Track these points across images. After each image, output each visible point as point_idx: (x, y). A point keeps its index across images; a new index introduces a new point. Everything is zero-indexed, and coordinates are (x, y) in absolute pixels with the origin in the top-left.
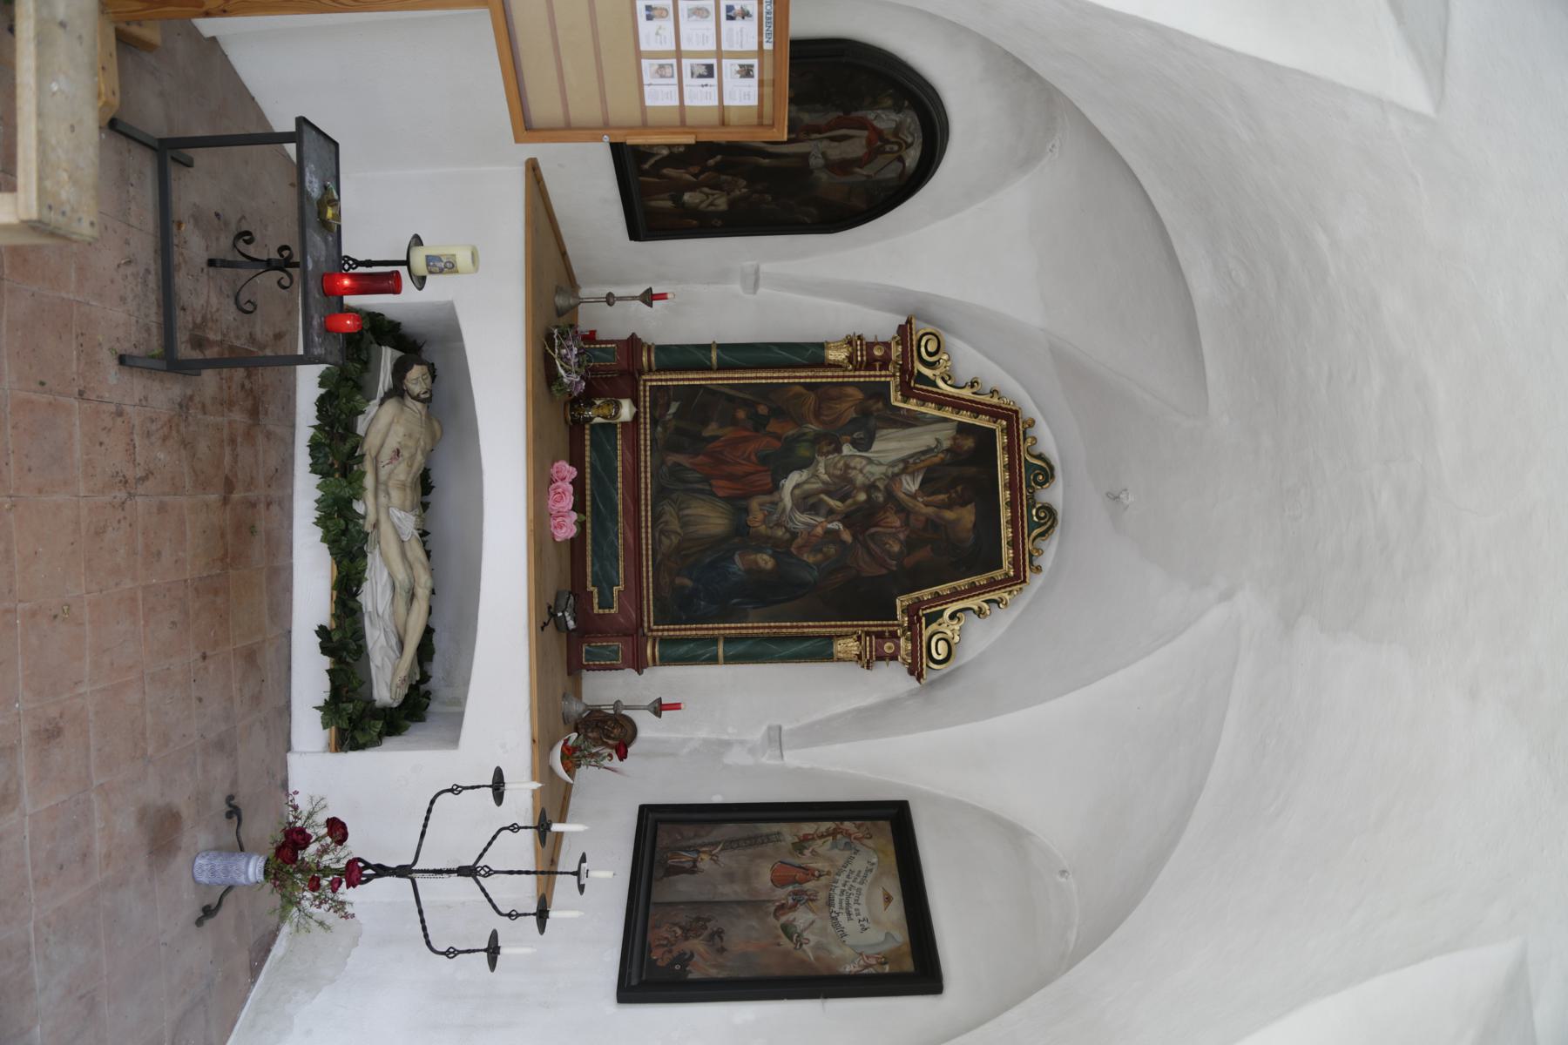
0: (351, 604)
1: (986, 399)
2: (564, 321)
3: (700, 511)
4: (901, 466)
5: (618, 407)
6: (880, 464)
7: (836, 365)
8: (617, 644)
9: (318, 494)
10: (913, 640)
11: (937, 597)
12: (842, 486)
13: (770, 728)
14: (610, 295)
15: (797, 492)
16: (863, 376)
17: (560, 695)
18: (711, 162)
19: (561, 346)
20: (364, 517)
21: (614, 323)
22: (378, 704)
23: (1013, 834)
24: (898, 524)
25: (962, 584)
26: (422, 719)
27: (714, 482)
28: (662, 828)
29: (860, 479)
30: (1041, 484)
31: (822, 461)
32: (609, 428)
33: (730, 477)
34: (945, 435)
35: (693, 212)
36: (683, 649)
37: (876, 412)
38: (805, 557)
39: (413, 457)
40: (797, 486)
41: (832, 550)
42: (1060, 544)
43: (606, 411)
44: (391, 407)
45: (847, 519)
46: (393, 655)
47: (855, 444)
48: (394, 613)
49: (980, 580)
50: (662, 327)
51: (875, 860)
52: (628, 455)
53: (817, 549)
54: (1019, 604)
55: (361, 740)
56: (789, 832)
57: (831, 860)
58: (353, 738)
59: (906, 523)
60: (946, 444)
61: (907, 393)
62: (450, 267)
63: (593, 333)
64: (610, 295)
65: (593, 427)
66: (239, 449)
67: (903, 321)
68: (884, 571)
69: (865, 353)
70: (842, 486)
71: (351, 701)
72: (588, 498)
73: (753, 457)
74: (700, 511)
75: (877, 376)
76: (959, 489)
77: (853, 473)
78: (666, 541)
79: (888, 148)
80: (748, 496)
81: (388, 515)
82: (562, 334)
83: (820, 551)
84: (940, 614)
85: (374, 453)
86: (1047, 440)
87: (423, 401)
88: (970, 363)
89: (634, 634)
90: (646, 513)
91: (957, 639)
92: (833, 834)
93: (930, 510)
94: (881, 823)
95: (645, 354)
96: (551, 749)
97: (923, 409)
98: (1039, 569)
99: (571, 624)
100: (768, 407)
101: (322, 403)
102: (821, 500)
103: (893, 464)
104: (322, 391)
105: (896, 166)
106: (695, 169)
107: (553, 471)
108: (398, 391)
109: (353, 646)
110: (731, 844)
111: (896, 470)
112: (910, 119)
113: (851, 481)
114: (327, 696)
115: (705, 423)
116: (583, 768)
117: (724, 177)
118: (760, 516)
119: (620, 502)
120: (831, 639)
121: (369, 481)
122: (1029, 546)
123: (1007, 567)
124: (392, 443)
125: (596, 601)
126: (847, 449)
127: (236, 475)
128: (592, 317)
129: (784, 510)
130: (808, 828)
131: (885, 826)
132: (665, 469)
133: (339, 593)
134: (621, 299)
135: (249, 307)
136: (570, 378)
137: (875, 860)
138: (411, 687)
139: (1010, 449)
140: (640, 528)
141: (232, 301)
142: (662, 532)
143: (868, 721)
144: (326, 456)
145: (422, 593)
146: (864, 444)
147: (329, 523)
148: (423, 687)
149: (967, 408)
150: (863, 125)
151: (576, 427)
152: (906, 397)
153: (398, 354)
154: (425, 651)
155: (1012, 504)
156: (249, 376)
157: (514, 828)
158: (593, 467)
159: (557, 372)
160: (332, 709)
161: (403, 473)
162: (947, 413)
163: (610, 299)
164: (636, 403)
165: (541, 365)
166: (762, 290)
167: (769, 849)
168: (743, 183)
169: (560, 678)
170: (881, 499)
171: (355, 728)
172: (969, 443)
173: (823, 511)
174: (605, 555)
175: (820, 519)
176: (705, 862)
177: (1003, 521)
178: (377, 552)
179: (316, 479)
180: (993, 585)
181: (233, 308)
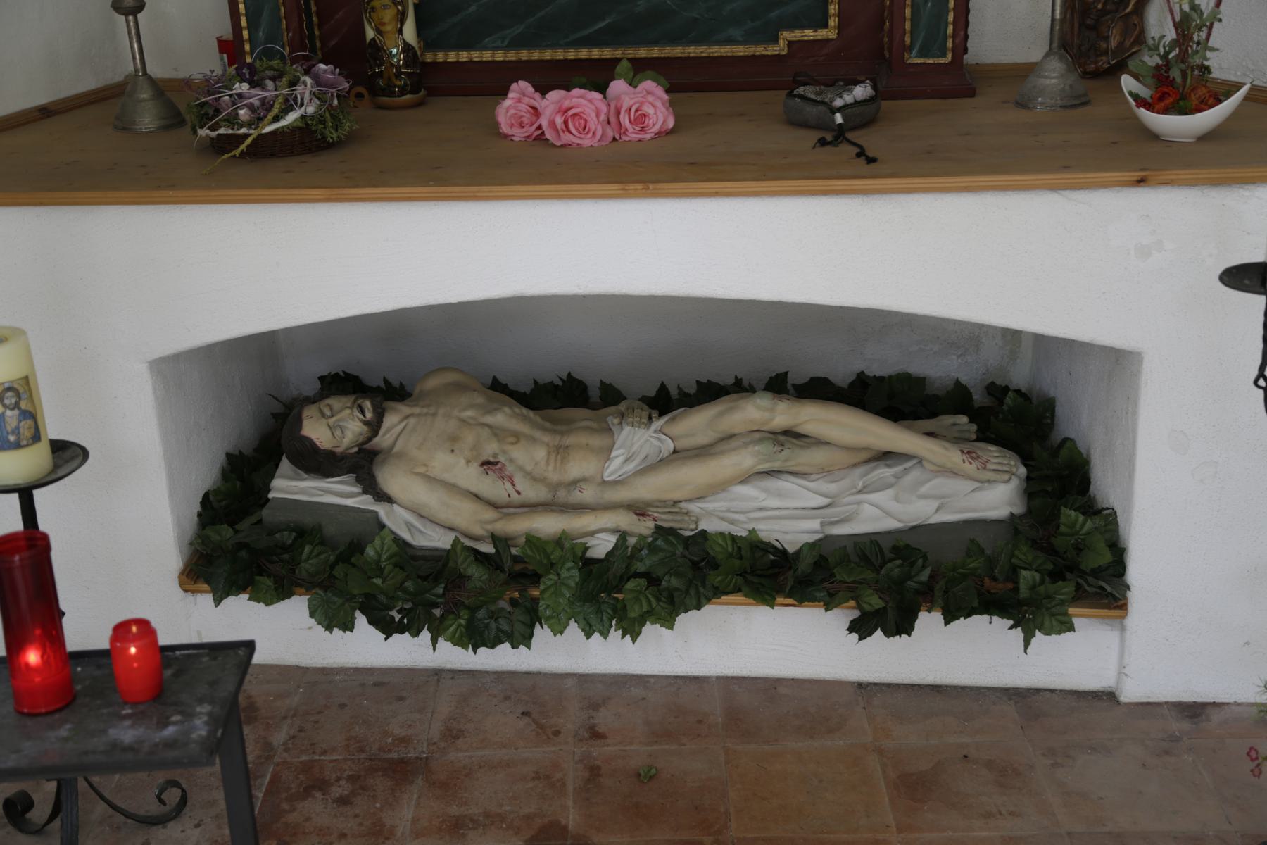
0: (804, 566)
9: (573, 630)
19: (233, 120)
20: (623, 536)
22: (1019, 509)
39: (497, 433)
43: (389, 15)
44: (392, 479)
46: (915, 474)
48: (825, 472)
55: (1107, 557)
58: (1097, 573)
63: (223, 46)
71: (1013, 572)
72: (584, 54)
81: (620, 479)
82: (207, 115)
85: (490, 514)
96: (1153, 137)
99: (861, 92)
101: (388, 628)
104: (361, 620)
107: (518, 134)
108: (362, 464)
109: (894, 568)
116: (1213, 60)
121: (548, 525)
124: (470, 477)
125: (809, 34)
127: (528, 817)
133: (780, 591)
135: (173, 796)
138: (984, 436)
141: (159, 833)
144: (494, 616)
145: (785, 413)
147: (634, 613)
148: (979, 398)
151: (428, 82)
153: (285, 465)
154: (896, 397)
156: (321, 785)
158: (516, 44)
159: (292, 129)
160: (1032, 613)
161: (532, 455)
171: (1074, 568)
178: (694, 507)
179: (542, 634)
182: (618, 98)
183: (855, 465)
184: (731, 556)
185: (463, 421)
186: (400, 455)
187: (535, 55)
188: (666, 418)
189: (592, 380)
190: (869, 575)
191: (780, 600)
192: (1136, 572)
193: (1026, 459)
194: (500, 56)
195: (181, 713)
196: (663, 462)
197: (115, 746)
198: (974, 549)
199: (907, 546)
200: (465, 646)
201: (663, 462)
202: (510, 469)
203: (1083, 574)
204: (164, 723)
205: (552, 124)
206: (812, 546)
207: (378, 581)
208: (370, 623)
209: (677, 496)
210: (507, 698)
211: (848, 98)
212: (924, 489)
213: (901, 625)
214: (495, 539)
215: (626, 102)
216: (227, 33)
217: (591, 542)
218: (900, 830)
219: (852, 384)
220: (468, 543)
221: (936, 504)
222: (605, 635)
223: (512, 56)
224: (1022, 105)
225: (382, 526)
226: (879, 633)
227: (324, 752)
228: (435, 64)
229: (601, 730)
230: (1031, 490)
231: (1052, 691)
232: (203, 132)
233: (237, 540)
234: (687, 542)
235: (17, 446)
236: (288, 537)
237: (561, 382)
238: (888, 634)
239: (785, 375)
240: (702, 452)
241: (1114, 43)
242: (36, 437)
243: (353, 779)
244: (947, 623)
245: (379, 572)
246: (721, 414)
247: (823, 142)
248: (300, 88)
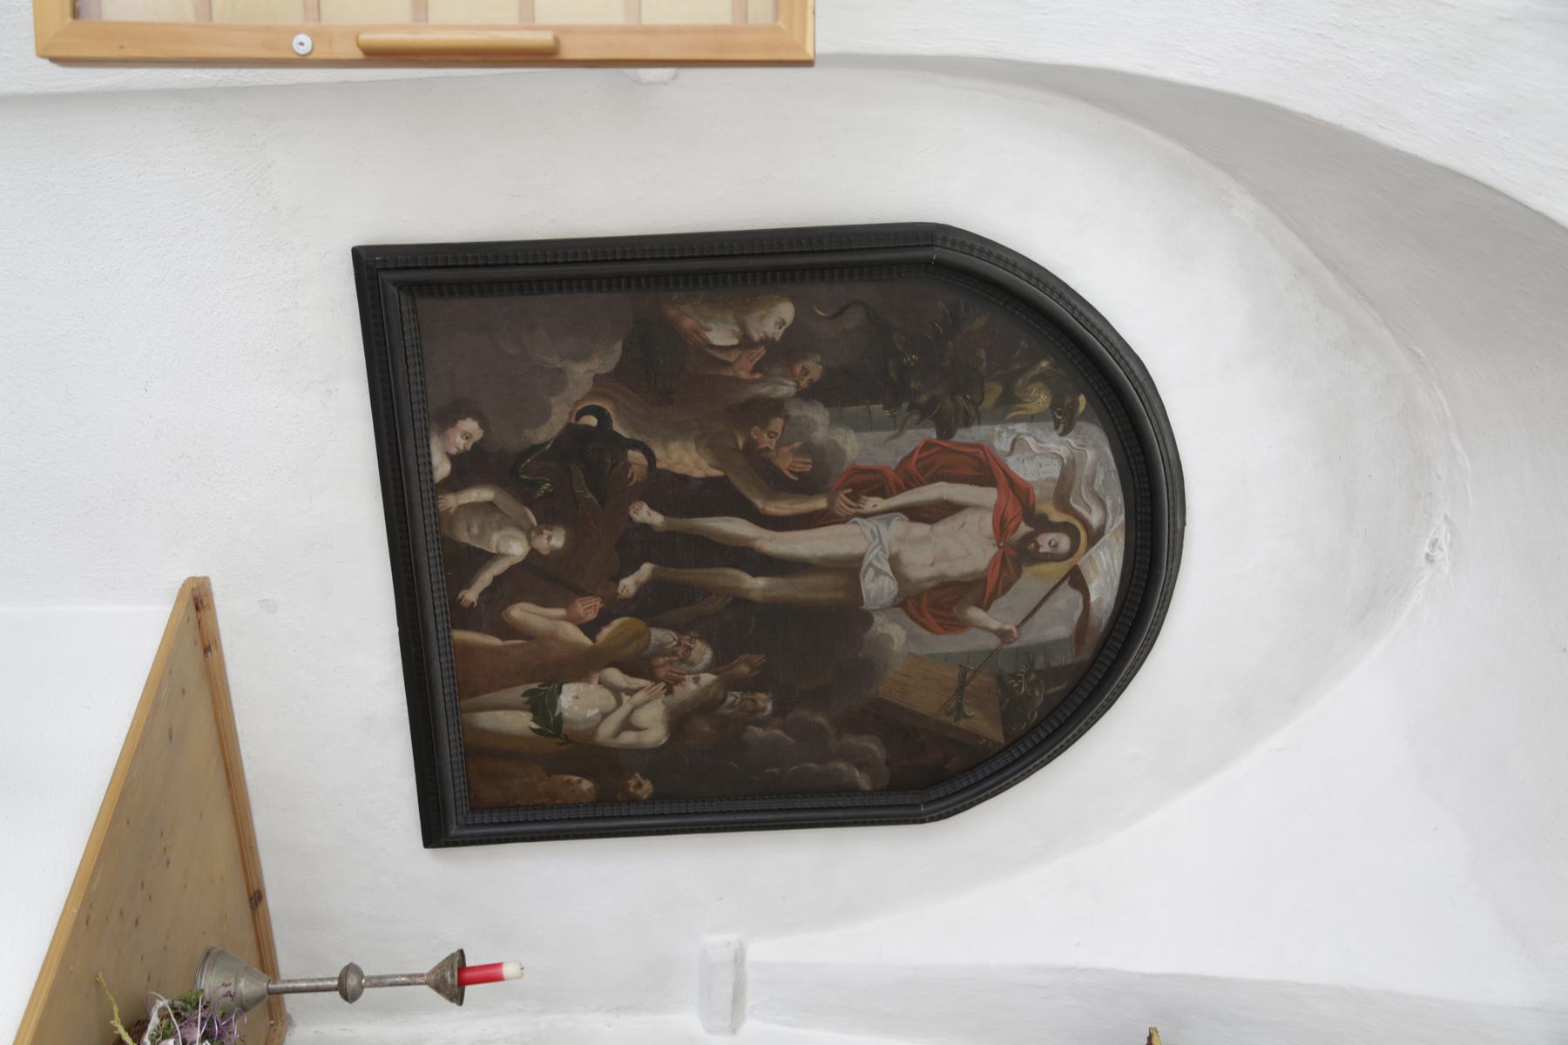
18: (628, 585)
79: (1045, 542)
106: (588, 608)
112: (1092, 449)
117: (658, 635)
150: (985, 470)
166: (750, 1025)
168: (703, 653)
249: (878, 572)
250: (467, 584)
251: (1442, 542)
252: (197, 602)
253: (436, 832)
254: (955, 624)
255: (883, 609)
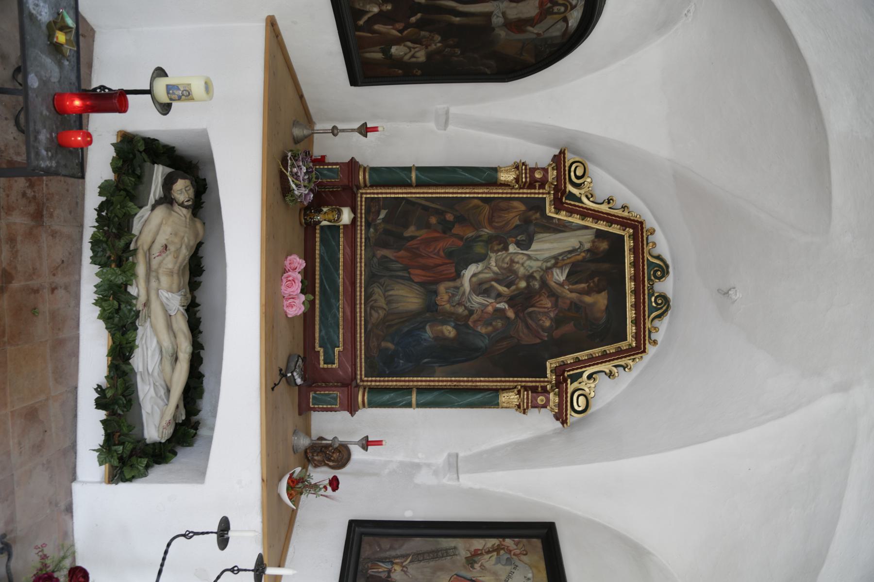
0: (124, 367)
1: (619, 213)
2: (301, 147)
3: (401, 292)
4: (553, 261)
5: (340, 213)
6: (537, 260)
7: (506, 185)
8: (337, 393)
9: (98, 280)
10: (560, 395)
11: (578, 361)
12: (508, 276)
13: (449, 455)
14: (334, 128)
15: (474, 279)
16: (526, 193)
17: (290, 431)
18: (413, 19)
19: (293, 166)
20: (136, 298)
21: (338, 149)
23: (637, 553)
24: (549, 305)
25: (597, 351)
26: (190, 444)
27: (411, 271)
28: (365, 539)
29: (522, 271)
30: (659, 278)
31: (493, 255)
32: (334, 229)
33: (424, 268)
34: (585, 239)
35: (398, 63)
36: (386, 397)
37: (532, 223)
38: (479, 329)
39: (178, 250)
40: (474, 275)
41: (499, 324)
42: (670, 323)
43: (330, 217)
44: (161, 211)
45: (511, 301)
46: (161, 403)
47: (518, 244)
48: (162, 371)
49: (611, 349)
50: (374, 153)
51: (530, 575)
52: (348, 250)
53: (488, 323)
54: (639, 365)
55: (128, 477)
56: (463, 546)
57: (495, 574)
58: (122, 472)
59: (555, 305)
60: (587, 246)
61: (559, 206)
62: (187, 95)
63: (323, 157)
64: (334, 128)
65: (322, 228)
66: (19, 246)
67: (557, 152)
68: (538, 341)
69: (529, 177)
70: (508, 276)
71: (123, 444)
72: (317, 281)
73: (442, 253)
74: (401, 292)
75: (536, 193)
76: (596, 279)
77: (516, 266)
78: (375, 315)
79: (556, 9)
80: (437, 282)
81: (159, 296)
82: (295, 157)
83: (491, 324)
84: (580, 375)
85: (146, 247)
86: (662, 244)
87: (186, 207)
88: (604, 184)
89: (349, 384)
90: (360, 294)
91: (593, 394)
92: (497, 549)
93: (574, 295)
94: (534, 540)
95: (361, 174)
96: (280, 480)
97: (570, 219)
98: (655, 342)
99: (299, 381)
100: (455, 214)
101: (100, 210)
102: (492, 286)
103: (547, 260)
104: (104, 199)
105: (561, 26)
106: (400, 26)
108: (167, 200)
110: (418, 557)
111: (549, 264)
113: (515, 273)
114: (103, 438)
115: (406, 226)
116: (303, 497)
117: (423, 33)
118: (446, 297)
119: (341, 284)
120: (497, 391)
121: (141, 270)
122: (648, 325)
123: (630, 340)
124: (161, 240)
125: (322, 358)
126: (512, 248)
127: (15, 268)
128: (322, 146)
129: (464, 293)
130: (478, 544)
131: (537, 543)
132: (375, 260)
134: (343, 131)
136: (301, 192)
137: (530, 575)
138: (177, 426)
139: (635, 250)
140: (355, 304)
142: (372, 308)
143: (523, 453)
144: (104, 250)
146: (526, 245)
147: (104, 304)
148: (194, 419)
149: (604, 219)
151: (309, 228)
152: (558, 210)
153: (169, 170)
155: (636, 292)
156: (32, 185)
157: (234, 570)
159: (290, 186)
160: (107, 450)
161: (170, 264)
162: (588, 222)
163: (334, 131)
164: (354, 210)
165: (277, 181)
166: (451, 127)
167: (446, 562)
168: (438, 38)
169: (291, 417)
170: (537, 286)
172: (604, 246)
173: (493, 294)
174: (330, 323)
175: (491, 301)
176: (397, 574)
177: (628, 305)
178: (148, 324)
179: (96, 269)
180: (620, 353)
181: (12, 129)
182: (299, 298)
183: (165, 381)
184: (127, 340)
185: (183, 237)
186: (170, 214)
187: (317, 264)
188: (184, 312)
189: (203, 278)
190: (120, 392)
191: (110, 358)
192: (123, 486)
193: (169, 441)
194: (317, 252)
195: (52, 156)
196: (165, 311)
197: (37, 133)
198: (130, 427)
199: (131, 405)
200: (91, 238)
201: (165, 311)
202: (164, 255)
203: (121, 468)
204: (47, 150)
205: (289, 276)
206: (133, 369)
207: (119, 206)
208: (102, 202)
209: (152, 317)
210: (70, 254)
211: (296, 377)
212: (156, 407)
213: (100, 404)
214: (135, 250)
215: (297, 301)
216: (327, 161)
217: (134, 286)
218: (12, 412)
219: (200, 373)
220: (134, 240)
221: (149, 411)
222: (95, 292)
223: (317, 256)
224: (295, 433)
225: (141, 208)
226: (97, 395)
227: (47, 185)
228: (316, 229)
229: (56, 292)
230: (155, 444)
231: (76, 458)
232: (289, 154)
233: (135, 153)
234: (133, 323)
235: (168, 93)
236: (138, 172)
237: (198, 270)
238: (97, 400)
239: (203, 349)
240: (170, 327)
241: (316, 458)
242: (171, 99)
243: (34, 197)
244: (101, 421)
245: (123, 207)
246: (184, 334)
247: (281, 370)
248: (303, 189)
249: (498, 17)
250: (360, 20)
251: (692, 11)
252: (272, 24)
253: (354, 82)
254: (524, 31)
255: (499, 27)
